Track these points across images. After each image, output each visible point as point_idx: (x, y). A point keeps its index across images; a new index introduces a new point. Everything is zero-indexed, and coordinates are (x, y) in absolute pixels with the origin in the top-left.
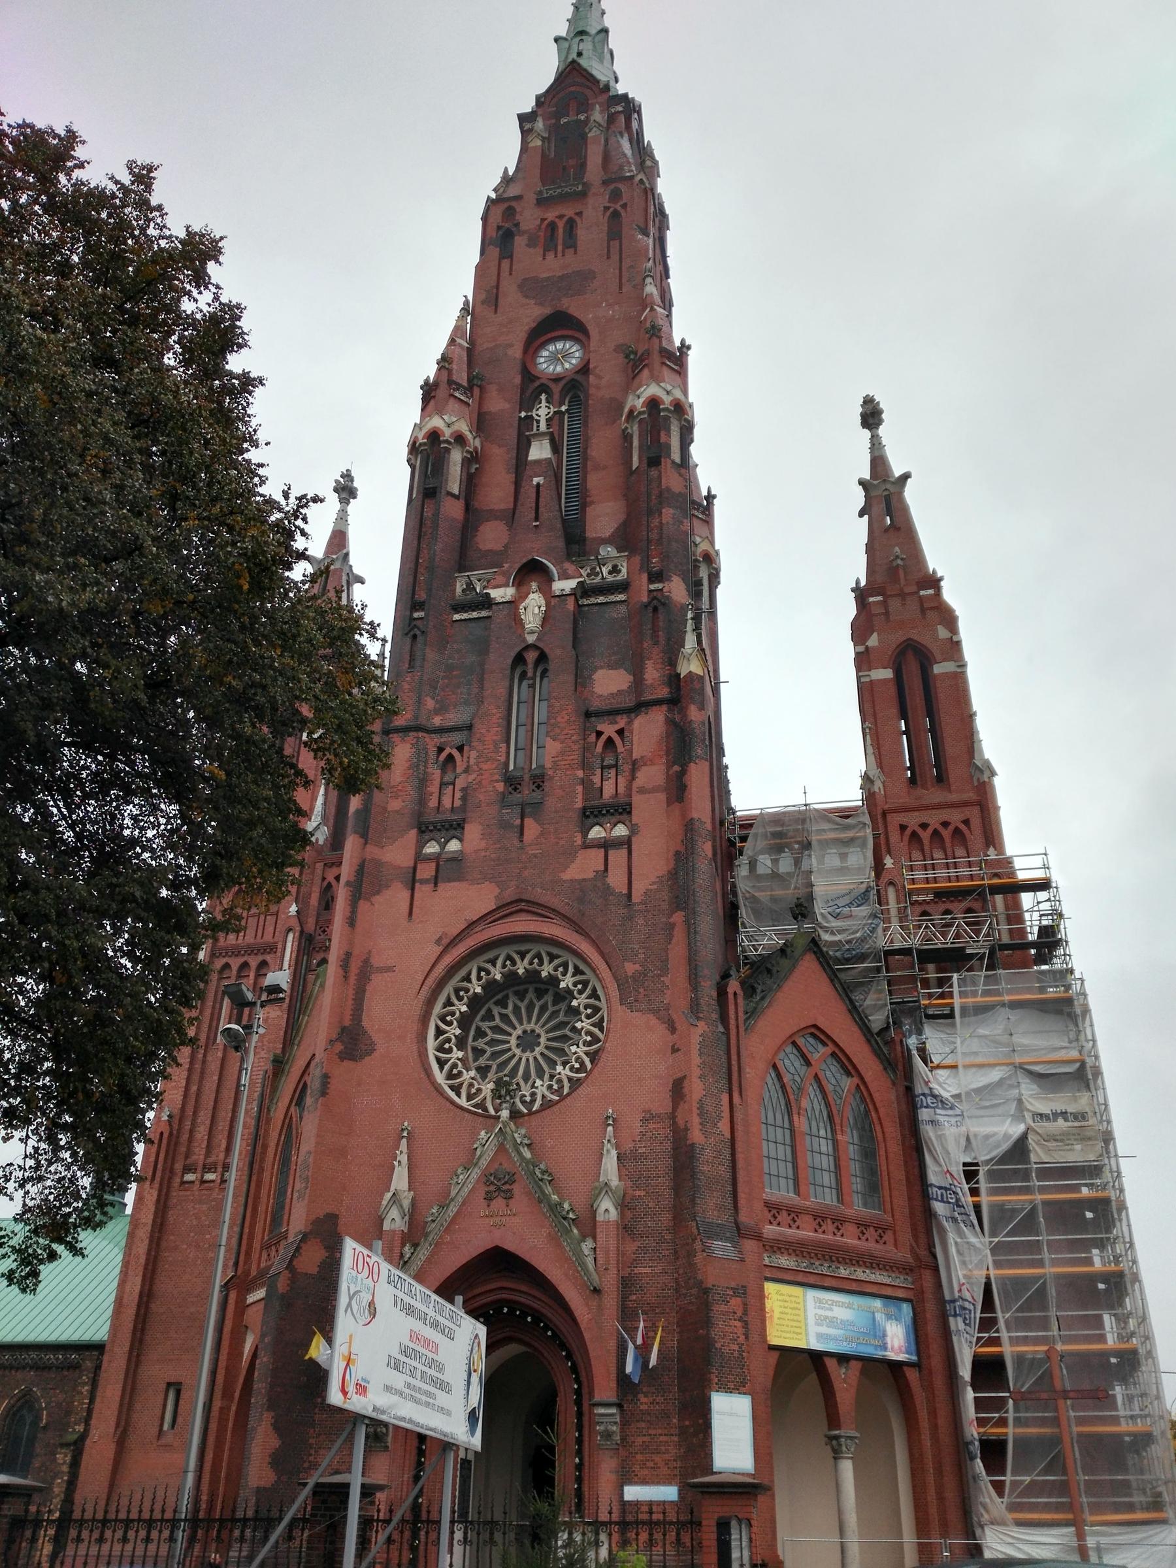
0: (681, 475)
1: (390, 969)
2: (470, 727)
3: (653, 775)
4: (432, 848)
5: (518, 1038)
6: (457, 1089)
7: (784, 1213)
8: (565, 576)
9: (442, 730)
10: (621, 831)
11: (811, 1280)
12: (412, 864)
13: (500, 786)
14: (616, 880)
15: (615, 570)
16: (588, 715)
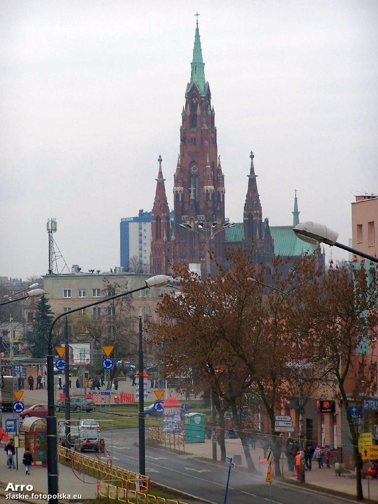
4: (182, 260)
10: (204, 259)
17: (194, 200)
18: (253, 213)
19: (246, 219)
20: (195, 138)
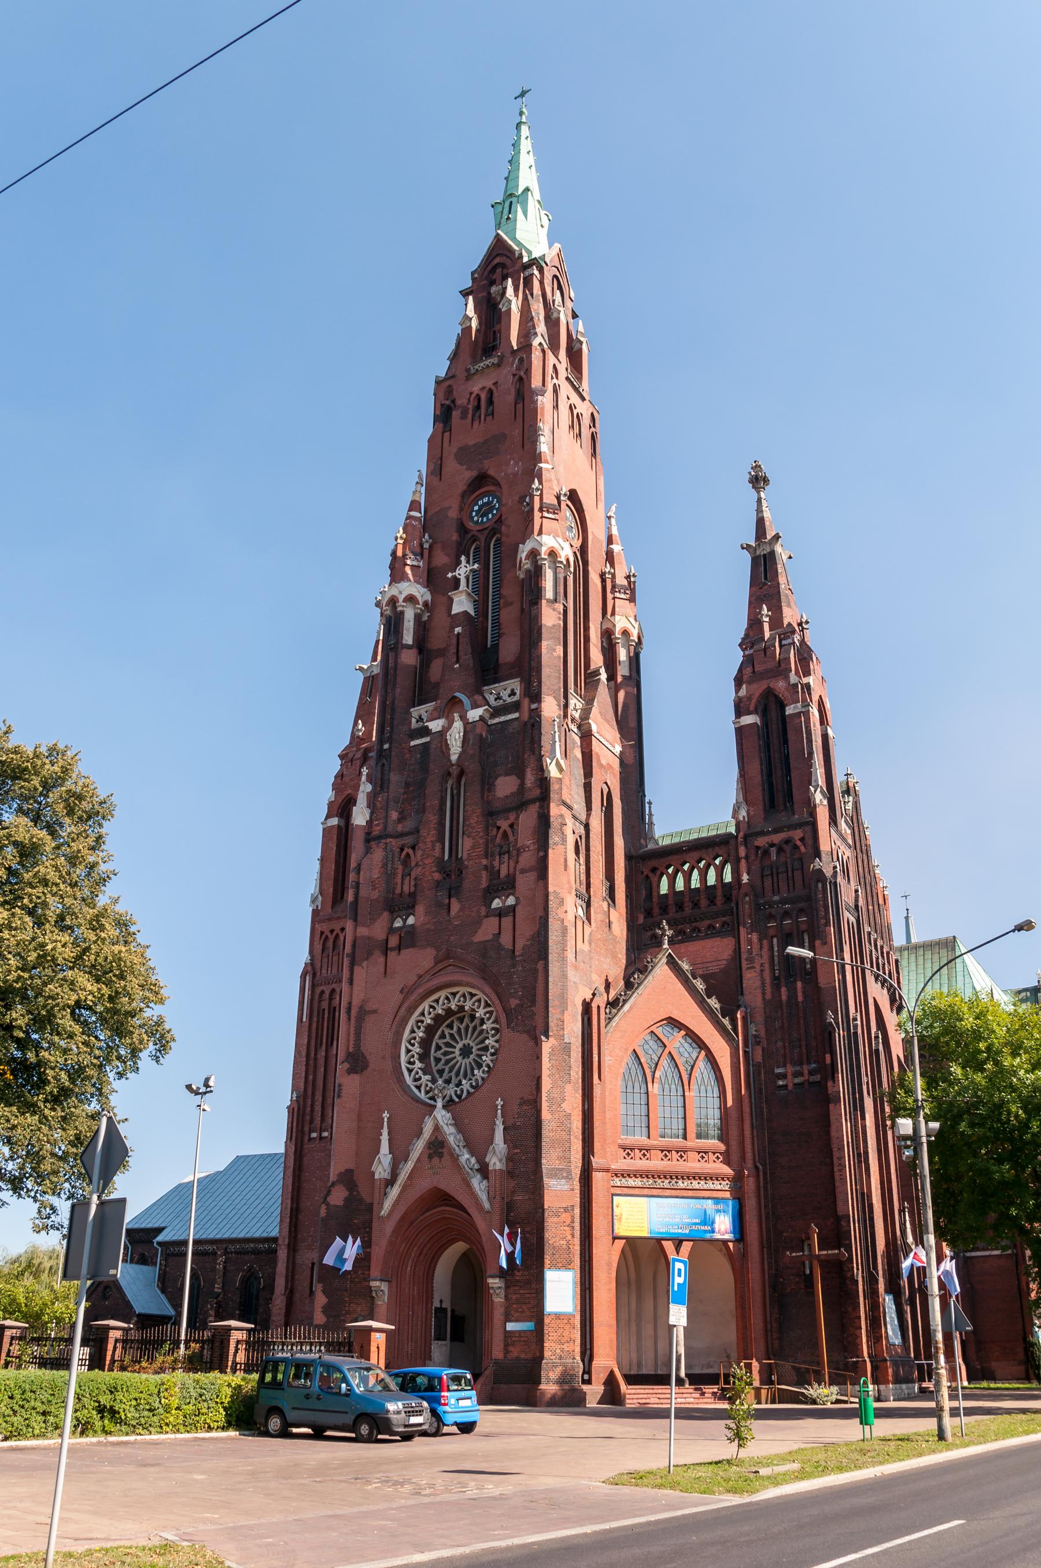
0: (554, 610)
1: (374, 1012)
2: (416, 831)
3: (527, 859)
4: (398, 923)
5: (461, 1049)
6: (418, 1088)
7: (637, 1151)
8: (475, 706)
9: (402, 835)
10: (511, 901)
11: (655, 1192)
12: (385, 937)
13: (437, 876)
14: (506, 940)
15: (513, 693)
16: (491, 814)
17: (474, 623)
18: (780, 685)
19: (748, 720)
20: (491, 392)
